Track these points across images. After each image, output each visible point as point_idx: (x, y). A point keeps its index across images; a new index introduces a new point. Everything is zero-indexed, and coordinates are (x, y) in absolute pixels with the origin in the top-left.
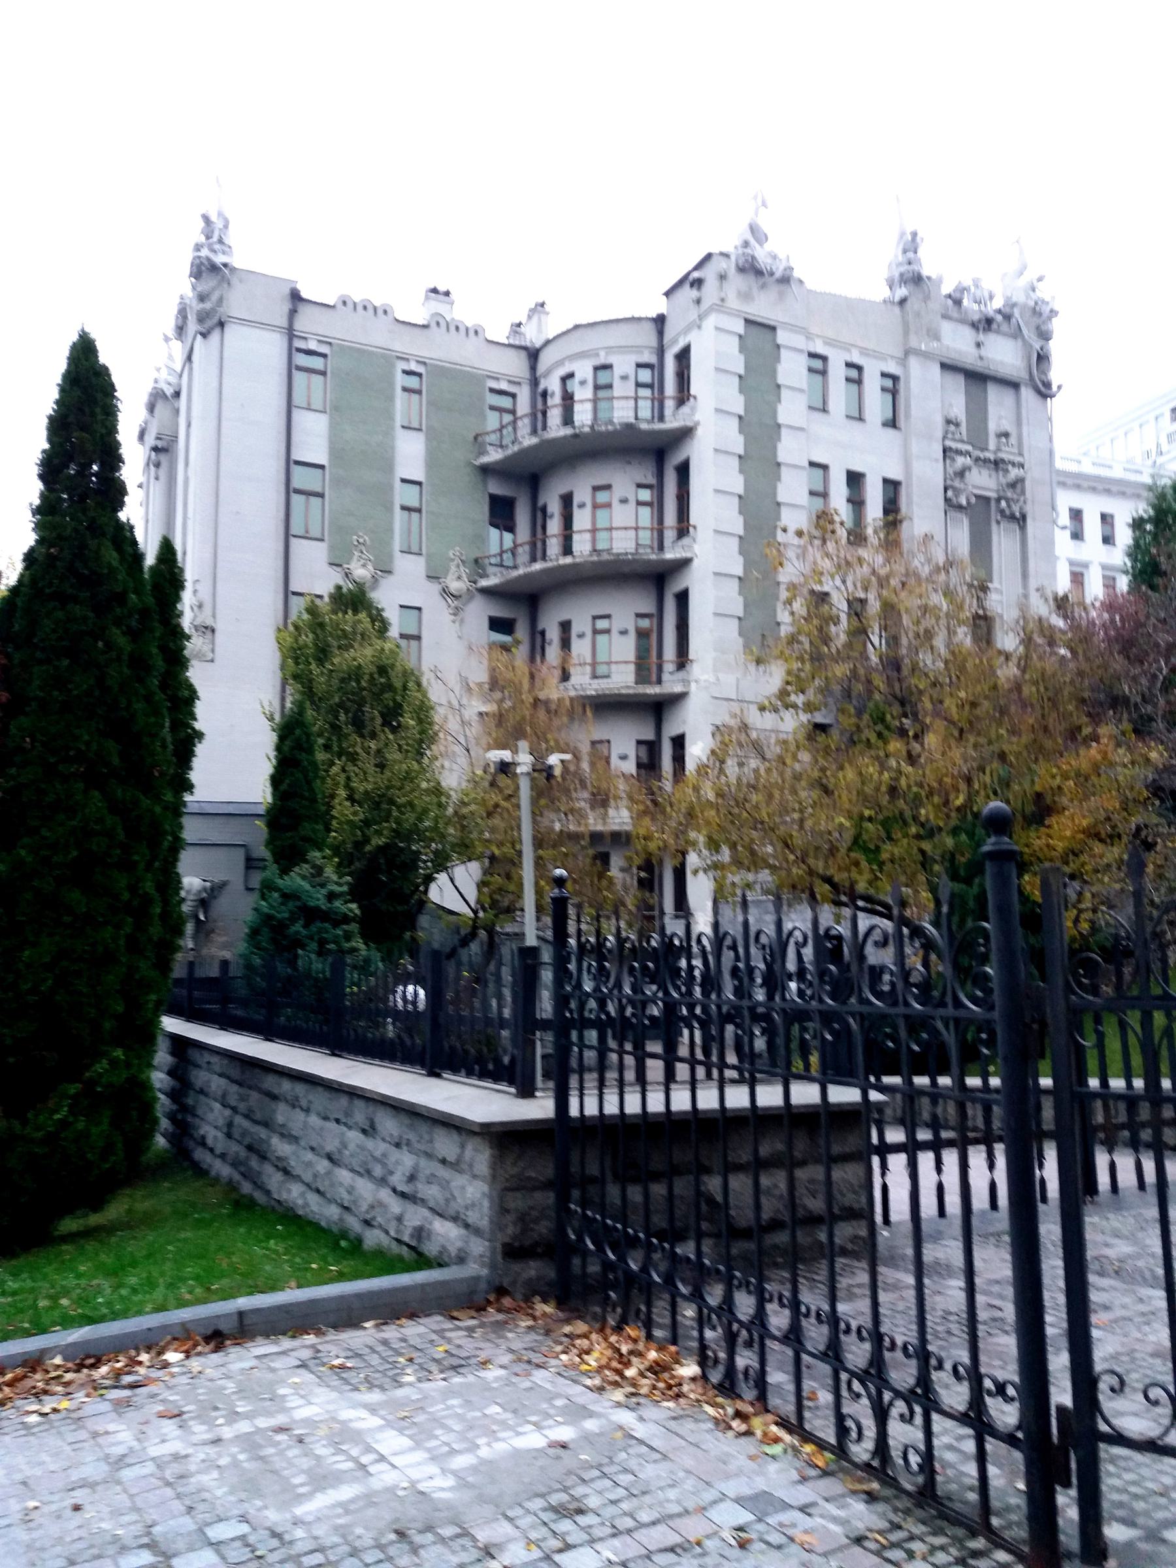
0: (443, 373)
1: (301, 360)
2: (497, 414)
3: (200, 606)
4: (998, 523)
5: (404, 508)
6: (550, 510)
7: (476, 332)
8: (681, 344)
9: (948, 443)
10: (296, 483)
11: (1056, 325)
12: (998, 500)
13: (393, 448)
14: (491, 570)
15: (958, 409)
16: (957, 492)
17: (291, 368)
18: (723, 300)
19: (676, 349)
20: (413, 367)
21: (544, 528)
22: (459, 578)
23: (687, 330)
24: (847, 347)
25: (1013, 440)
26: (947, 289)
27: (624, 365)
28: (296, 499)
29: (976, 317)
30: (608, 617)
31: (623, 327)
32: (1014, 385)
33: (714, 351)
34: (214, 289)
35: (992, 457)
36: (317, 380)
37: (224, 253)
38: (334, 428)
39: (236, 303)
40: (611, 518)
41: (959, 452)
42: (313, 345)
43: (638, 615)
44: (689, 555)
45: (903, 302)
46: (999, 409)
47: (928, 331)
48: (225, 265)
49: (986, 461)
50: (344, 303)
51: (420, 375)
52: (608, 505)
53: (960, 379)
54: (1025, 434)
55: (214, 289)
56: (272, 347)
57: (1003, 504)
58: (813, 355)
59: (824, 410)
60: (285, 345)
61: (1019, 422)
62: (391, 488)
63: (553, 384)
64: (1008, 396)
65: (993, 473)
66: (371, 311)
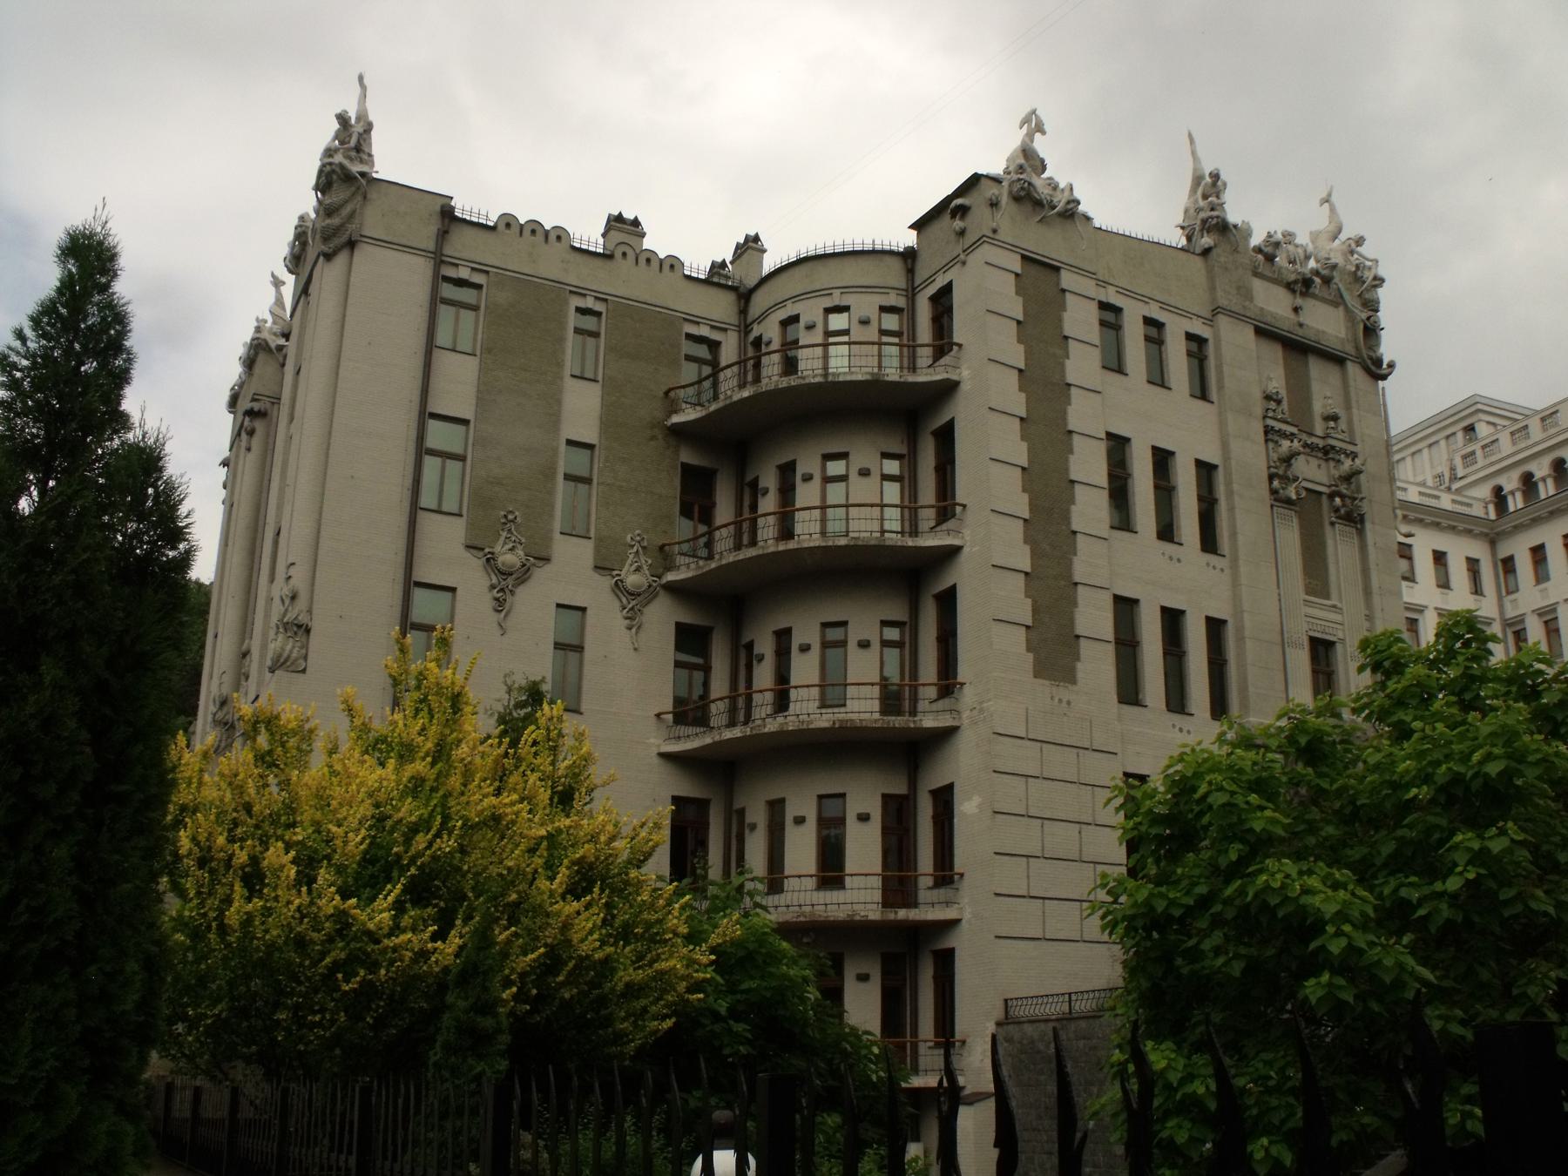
1: (448, 291)
2: (695, 366)
3: (293, 598)
4: (1332, 524)
5: (568, 477)
6: (762, 484)
7: (672, 266)
8: (940, 282)
9: (1270, 422)
10: (431, 442)
11: (1382, 293)
12: (1331, 496)
13: (559, 402)
14: (680, 560)
15: (1277, 384)
16: (1287, 480)
17: (436, 301)
18: (995, 231)
19: (932, 290)
20: (589, 303)
21: (754, 507)
22: (638, 569)
23: (946, 268)
25: (1343, 425)
26: (1256, 239)
27: (867, 305)
28: (431, 463)
29: (1292, 277)
30: (844, 624)
31: (863, 263)
32: (1338, 360)
33: (986, 292)
35: (1321, 443)
36: (467, 316)
37: (361, 161)
38: (483, 370)
39: (373, 221)
40: (850, 498)
41: (1284, 435)
42: (464, 273)
43: (884, 623)
44: (957, 542)
45: (1206, 252)
46: (1324, 387)
48: (363, 174)
50: (508, 225)
51: (598, 314)
52: (843, 478)
54: (1355, 419)
55: (346, 202)
56: (414, 275)
57: (1338, 500)
58: (1104, 306)
60: (429, 273)
61: (1348, 407)
62: (555, 451)
63: (770, 330)
64: (1333, 372)
66: (540, 237)
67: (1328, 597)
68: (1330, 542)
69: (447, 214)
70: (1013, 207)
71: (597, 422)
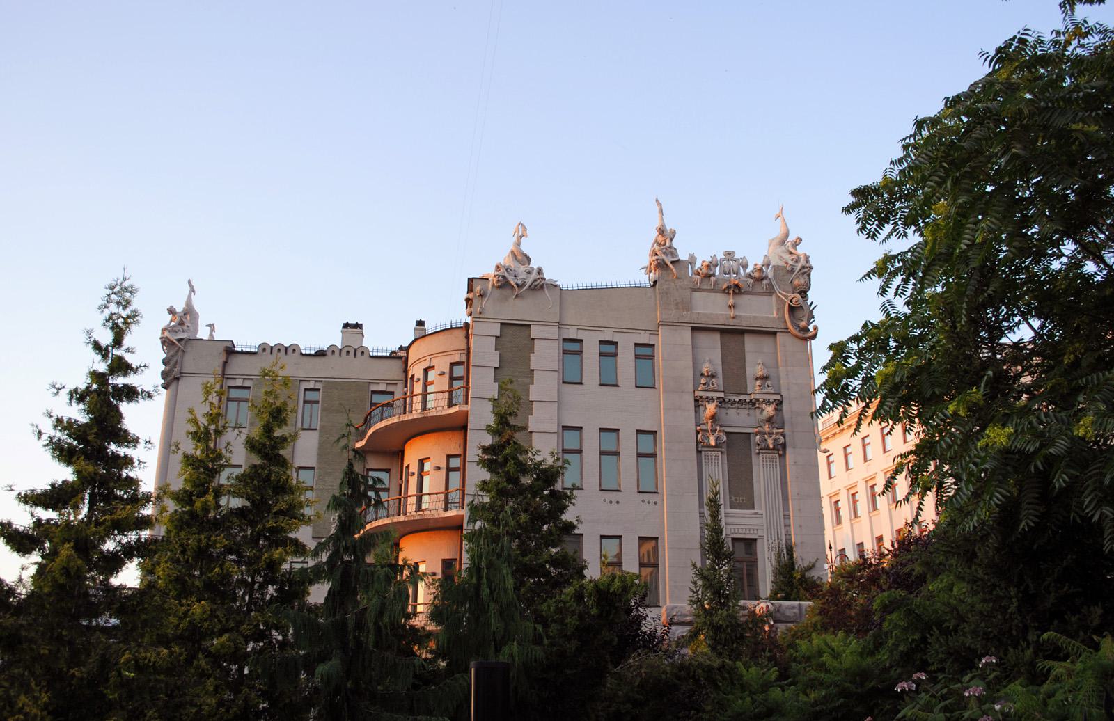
0: (332, 386)
20: (311, 385)
24: (600, 329)
27: (442, 364)
31: (440, 336)
32: (774, 334)
34: (173, 356)
35: (748, 398)
39: (189, 364)
42: (239, 382)
47: (677, 304)
48: (180, 340)
49: (741, 402)
51: (319, 390)
53: (717, 336)
54: (782, 375)
59: (581, 383)
64: (767, 340)
65: (752, 412)
67: (753, 508)
68: (754, 468)
69: (230, 350)
70: (497, 292)
71: (316, 454)
